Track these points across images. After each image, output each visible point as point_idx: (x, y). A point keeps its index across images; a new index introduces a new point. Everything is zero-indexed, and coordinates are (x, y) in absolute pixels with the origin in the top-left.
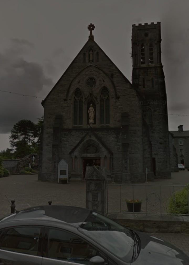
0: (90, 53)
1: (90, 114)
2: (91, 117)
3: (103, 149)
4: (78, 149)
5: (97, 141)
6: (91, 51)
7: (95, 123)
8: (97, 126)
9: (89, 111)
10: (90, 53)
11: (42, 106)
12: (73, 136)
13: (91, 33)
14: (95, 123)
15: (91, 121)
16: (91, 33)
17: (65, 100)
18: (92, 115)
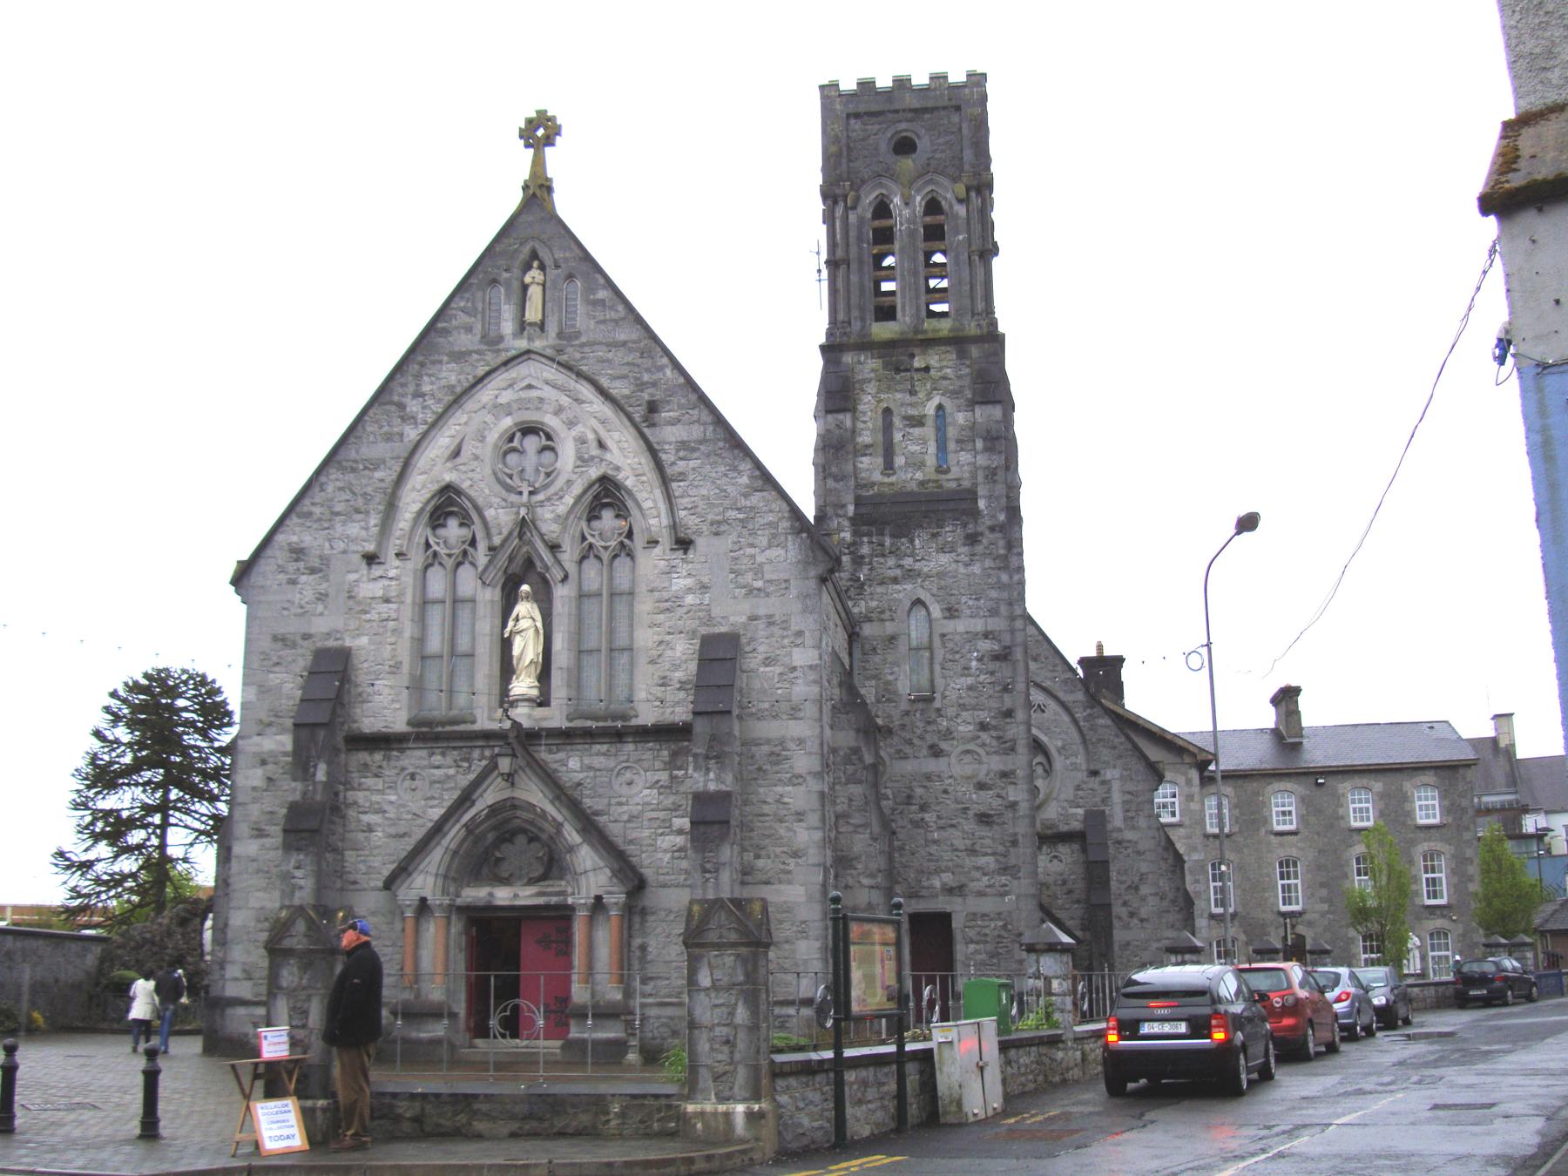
0: (527, 279)
1: (517, 645)
2: (519, 659)
3: (586, 857)
4: (436, 857)
5: (550, 809)
6: (535, 264)
7: (543, 701)
8: (554, 717)
9: (511, 623)
10: (527, 279)
11: (237, 592)
12: (413, 777)
13: (538, 164)
14: (543, 701)
15: (523, 685)
16: (538, 164)
17: (371, 559)
18: (526, 648)
